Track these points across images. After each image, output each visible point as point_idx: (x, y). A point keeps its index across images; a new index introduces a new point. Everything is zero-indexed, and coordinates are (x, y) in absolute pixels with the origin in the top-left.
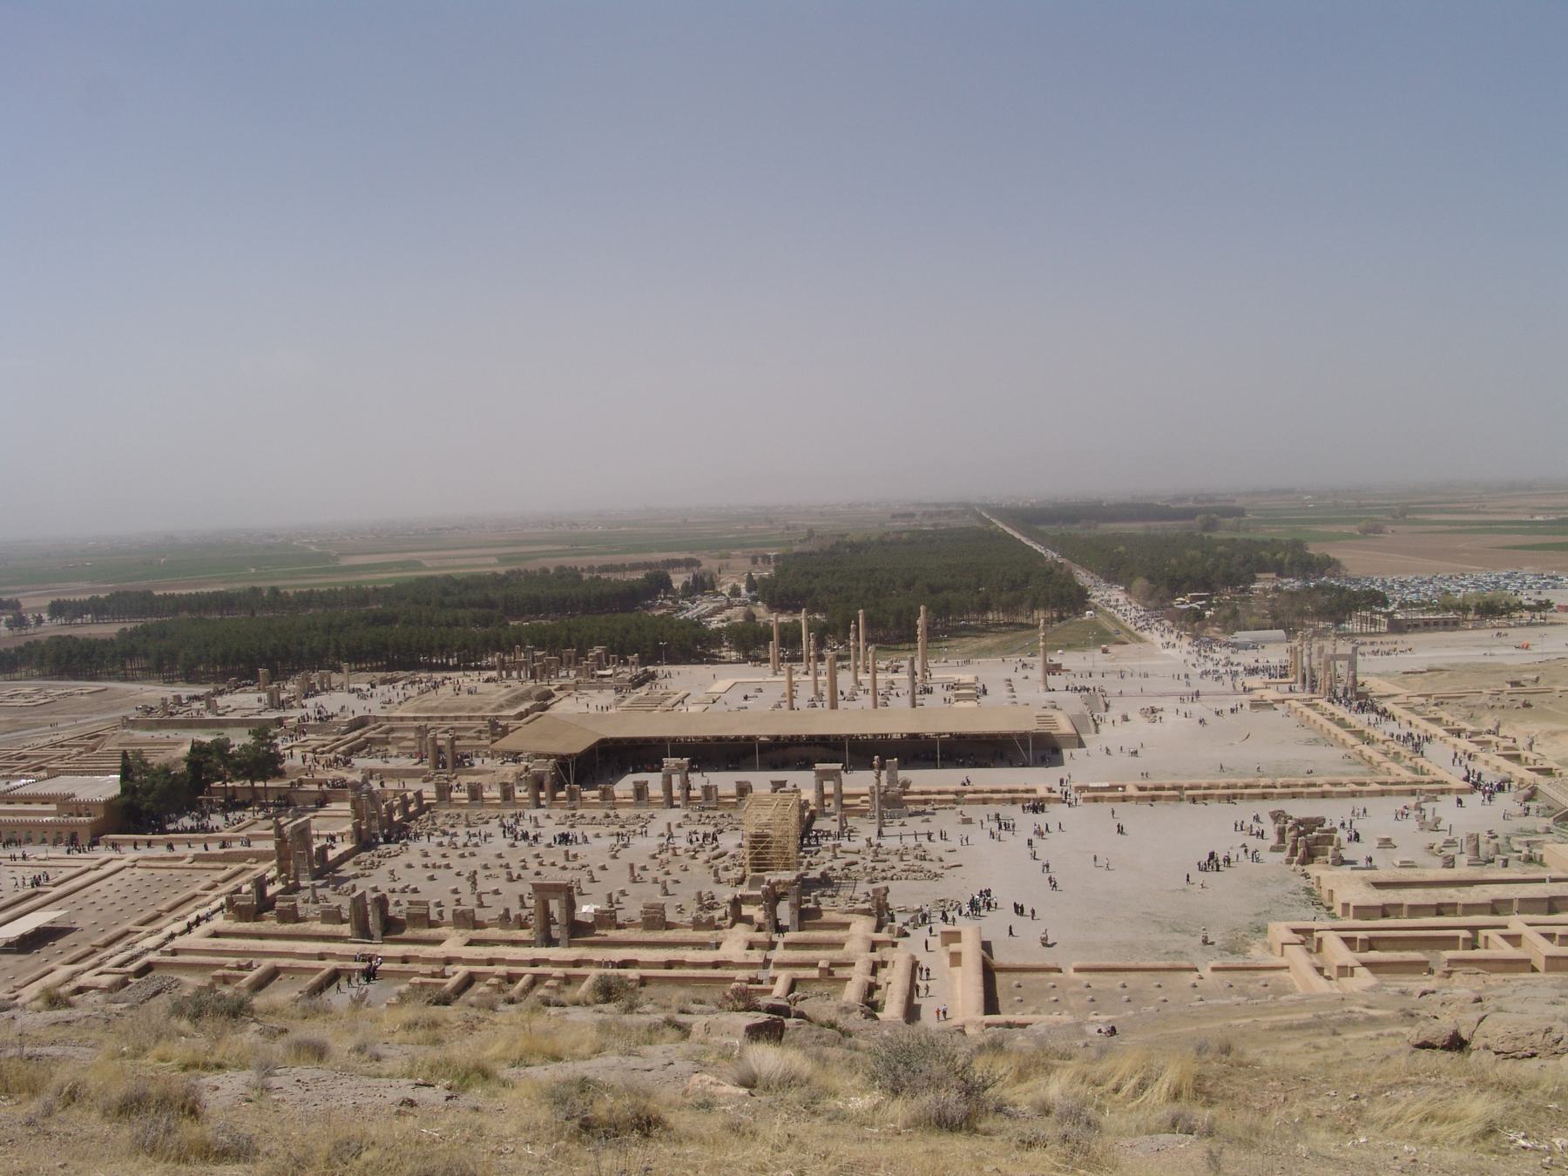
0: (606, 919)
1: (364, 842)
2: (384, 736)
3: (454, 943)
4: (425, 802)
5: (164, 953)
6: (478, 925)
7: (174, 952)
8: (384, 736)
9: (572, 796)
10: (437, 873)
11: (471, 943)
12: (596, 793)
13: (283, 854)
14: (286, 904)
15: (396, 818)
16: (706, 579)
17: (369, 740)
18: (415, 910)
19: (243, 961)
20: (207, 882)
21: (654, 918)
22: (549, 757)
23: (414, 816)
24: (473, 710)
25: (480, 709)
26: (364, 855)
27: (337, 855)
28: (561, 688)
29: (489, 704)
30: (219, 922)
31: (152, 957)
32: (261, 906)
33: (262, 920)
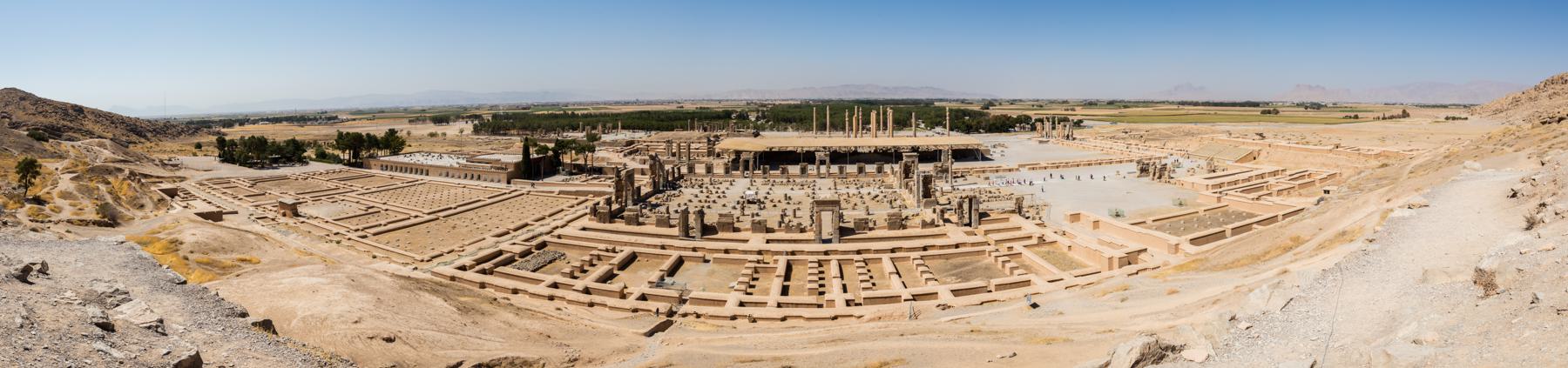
1: (656, 190)
3: (757, 241)
6: (769, 230)
9: (765, 173)
10: (711, 204)
11: (768, 242)
12: (779, 172)
14: (632, 213)
15: (670, 179)
18: (724, 220)
19: (610, 247)
21: (895, 222)
22: (751, 152)
25: (690, 138)
26: (660, 195)
32: (613, 216)
33: (615, 222)
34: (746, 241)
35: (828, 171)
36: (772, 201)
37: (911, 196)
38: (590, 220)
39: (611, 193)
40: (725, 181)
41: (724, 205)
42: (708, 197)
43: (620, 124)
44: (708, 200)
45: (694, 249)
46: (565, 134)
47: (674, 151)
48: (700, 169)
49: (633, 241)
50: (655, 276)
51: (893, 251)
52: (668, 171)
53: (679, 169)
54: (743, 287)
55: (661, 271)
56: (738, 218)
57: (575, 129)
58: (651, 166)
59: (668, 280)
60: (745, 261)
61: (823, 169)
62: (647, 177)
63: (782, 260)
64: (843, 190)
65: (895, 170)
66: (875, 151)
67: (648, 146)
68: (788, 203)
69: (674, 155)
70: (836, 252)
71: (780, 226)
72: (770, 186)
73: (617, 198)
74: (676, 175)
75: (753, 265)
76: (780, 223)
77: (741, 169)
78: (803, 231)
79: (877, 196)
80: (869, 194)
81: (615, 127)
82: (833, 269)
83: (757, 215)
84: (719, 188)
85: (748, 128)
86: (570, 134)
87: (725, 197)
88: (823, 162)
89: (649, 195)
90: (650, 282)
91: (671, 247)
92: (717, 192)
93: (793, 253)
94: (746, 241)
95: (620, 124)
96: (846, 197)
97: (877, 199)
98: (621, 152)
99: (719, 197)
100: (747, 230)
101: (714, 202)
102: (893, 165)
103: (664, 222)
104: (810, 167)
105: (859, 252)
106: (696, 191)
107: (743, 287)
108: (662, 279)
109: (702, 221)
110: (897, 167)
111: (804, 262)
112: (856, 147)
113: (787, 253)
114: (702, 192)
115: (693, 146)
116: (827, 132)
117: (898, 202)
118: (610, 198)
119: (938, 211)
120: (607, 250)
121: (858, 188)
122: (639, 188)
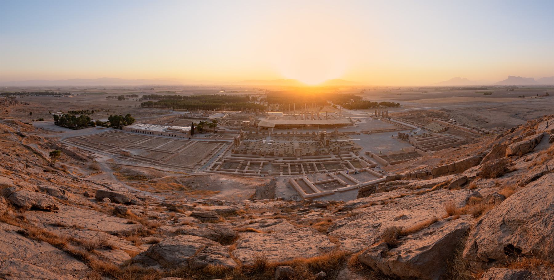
0: (307, 154)
11: (284, 159)
17: (227, 123)
45: (265, 161)
63: (289, 164)
70: (302, 162)
80: (310, 143)
82: (302, 166)
91: (260, 160)
105: (307, 162)
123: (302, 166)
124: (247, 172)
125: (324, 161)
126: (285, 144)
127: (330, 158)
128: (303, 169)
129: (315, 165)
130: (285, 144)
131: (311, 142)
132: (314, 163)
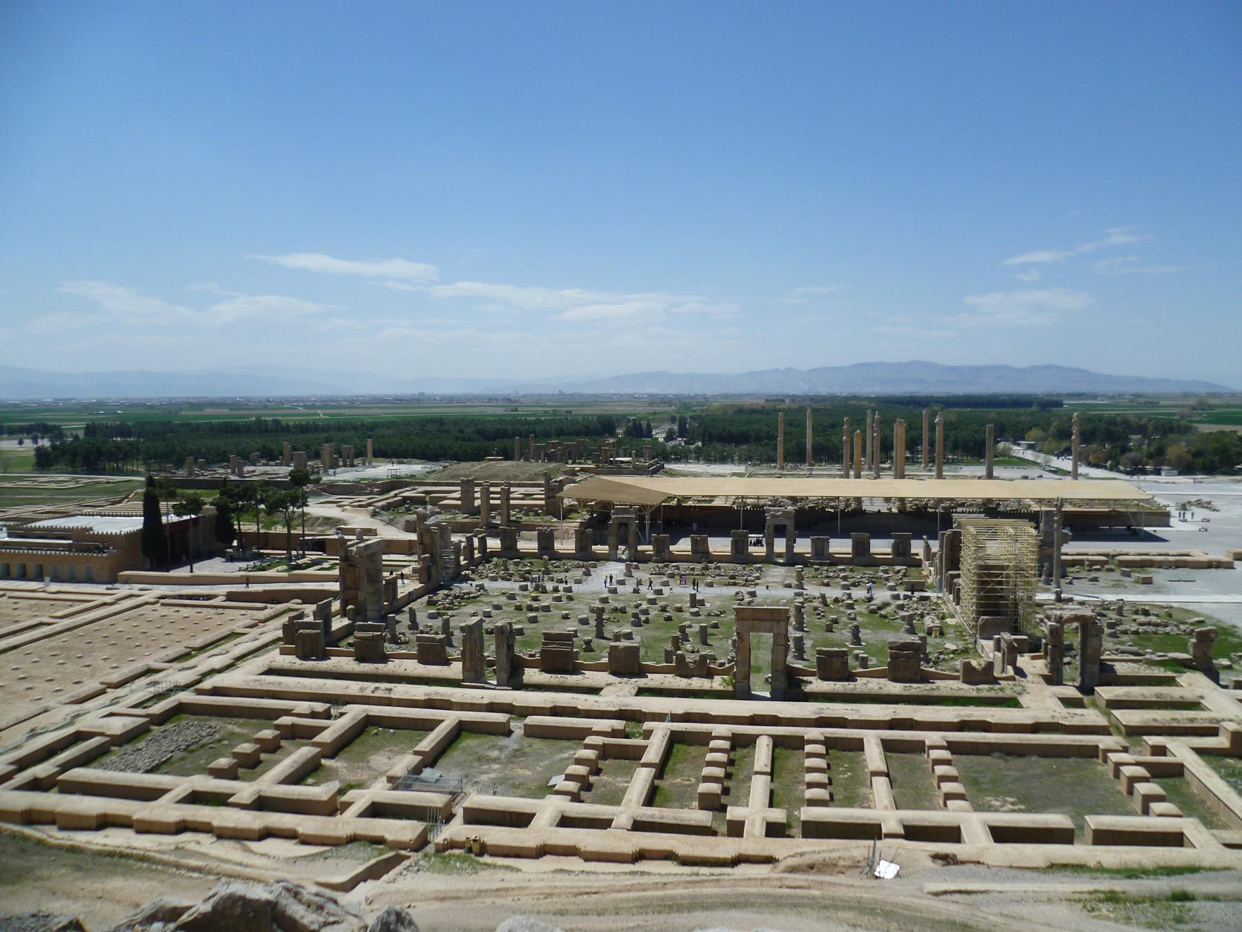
2: (423, 495)
4: (488, 550)
5: (201, 692)
7: (216, 691)
8: (423, 495)
11: (641, 692)
13: (348, 582)
14: (370, 634)
15: (463, 563)
16: (644, 423)
17: (405, 498)
19: (319, 707)
20: (249, 622)
22: (631, 506)
23: (478, 563)
24: (508, 478)
27: (406, 593)
28: (582, 470)
29: (523, 473)
30: (275, 657)
31: (187, 697)
34: (595, 691)
35: (790, 547)
36: (664, 609)
37: (958, 607)
38: (283, 652)
39: (334, 595)
40: (578, 567)
41: (566, 617)
42: (535, 599)
43: (369, 442)
44: (535, 604)
45: (492, 707)
46: (246, 469)
47: (477, 503)
48: (527, 544)
49: (368, 693)
50: (403, 763)
51: (894, 724)
52: (458, 545)
53: (483, 542)
54: (572, 786)
55: (416, 753)
56: (588, 643)
57: (270, 456)
58: (421, 536)
59: (427, 773)
60: (590, 732)
61: (780, 545)
62: (415, 558)
63: (660, 732)
64: (812, 590)
65: (933, 550)
66: (902, 511)
67: (427, 492)
68: (697, 614)
69: (475, 512)
71: (668, 660)
72: (665, 579)
73: (344, 604)
74: (477, 555)
75: (599, 740)
76: (668, 656)
77: (612, 539)
78: (709, 674)
79: (886, 605)
81: (360, 453)
82: (762, 755)
83: (629, 636)
84: (560, 581)
85: (639, 455)
86: (260, 469)
87: (570, 599)
88: (780, 531)
89: (412, 597)
90: (391, 779)
91: (446, 705)
92: (556, 590)
93: (687, 717)
94: (595, 691)
95: (369, 442)
96: (816, 604)
97: (883, 612)
98: (370, 505)
99: (559, 599)
100: (599, 668)
101: (547, 609)
102: (931, 542)
103: (432, 653)
104: (753, 537)
106: (513, 586)
107: (572, 786)
108: (417, 770)
109: (510, 647)
110: (935, 546)
111: (704, 738)
112: (859, 500)
113: (675, 718)
114: (524, 588)
115: (517, 492)
116: (806, 466)
117: (928, 621)
118: (329, 605)
119: (1003, 645)
120: (314, 715)
121: (846, 587)
122: (392, 584)
123: (762, 755)
124: (262, 804)
125: (963, 726)
126: (702, 603)
127: (1013, 703)
128: (759, 787)
129: (874, 756)
130: (695, 602)
131: (881, 595)
132: (872, 741)
